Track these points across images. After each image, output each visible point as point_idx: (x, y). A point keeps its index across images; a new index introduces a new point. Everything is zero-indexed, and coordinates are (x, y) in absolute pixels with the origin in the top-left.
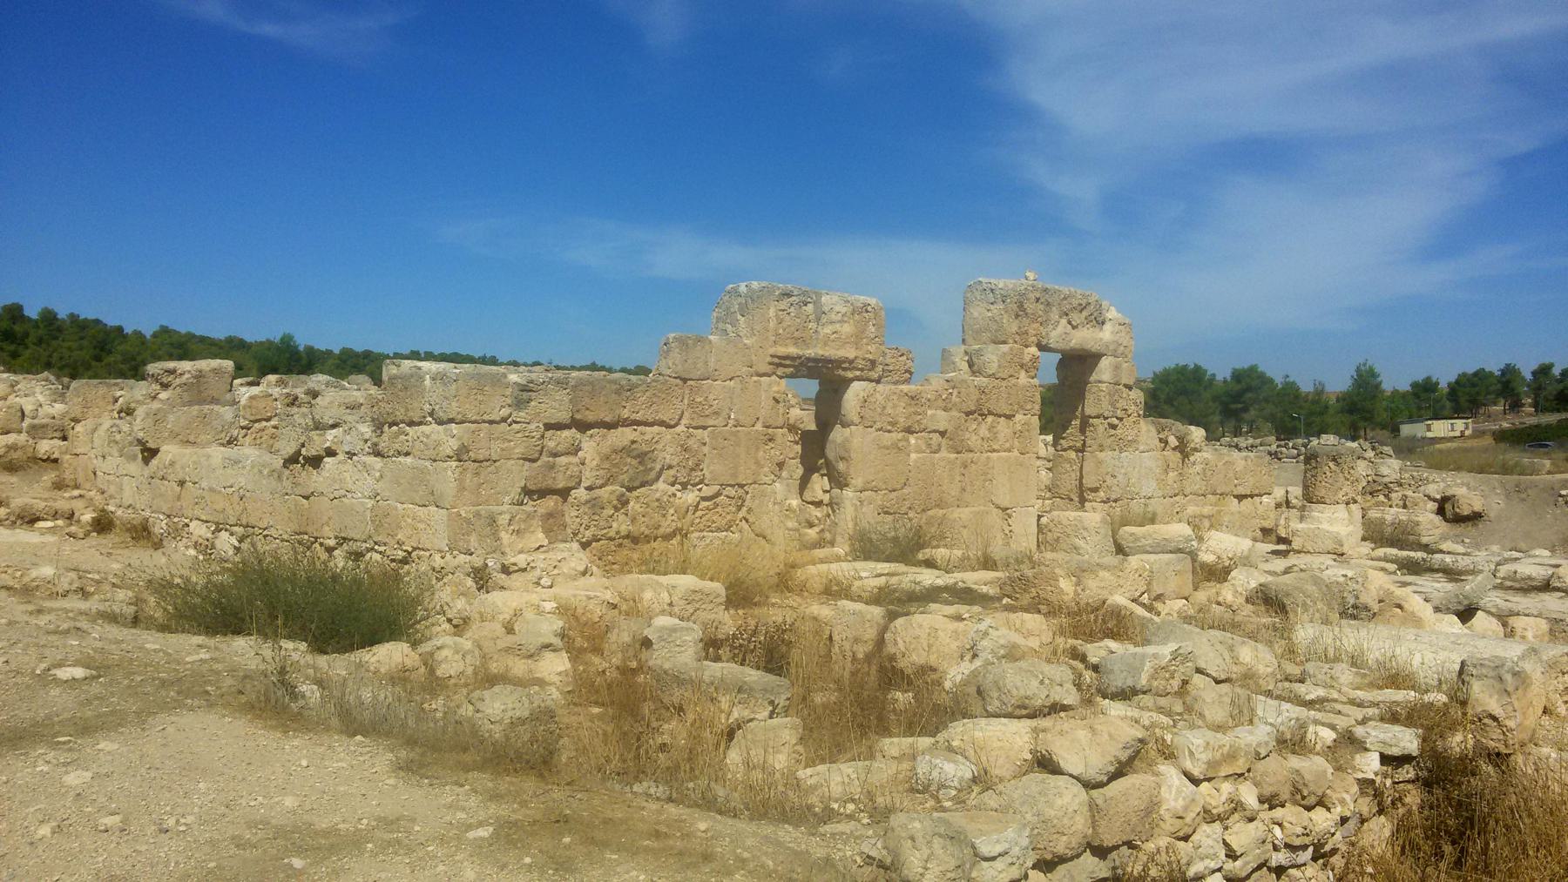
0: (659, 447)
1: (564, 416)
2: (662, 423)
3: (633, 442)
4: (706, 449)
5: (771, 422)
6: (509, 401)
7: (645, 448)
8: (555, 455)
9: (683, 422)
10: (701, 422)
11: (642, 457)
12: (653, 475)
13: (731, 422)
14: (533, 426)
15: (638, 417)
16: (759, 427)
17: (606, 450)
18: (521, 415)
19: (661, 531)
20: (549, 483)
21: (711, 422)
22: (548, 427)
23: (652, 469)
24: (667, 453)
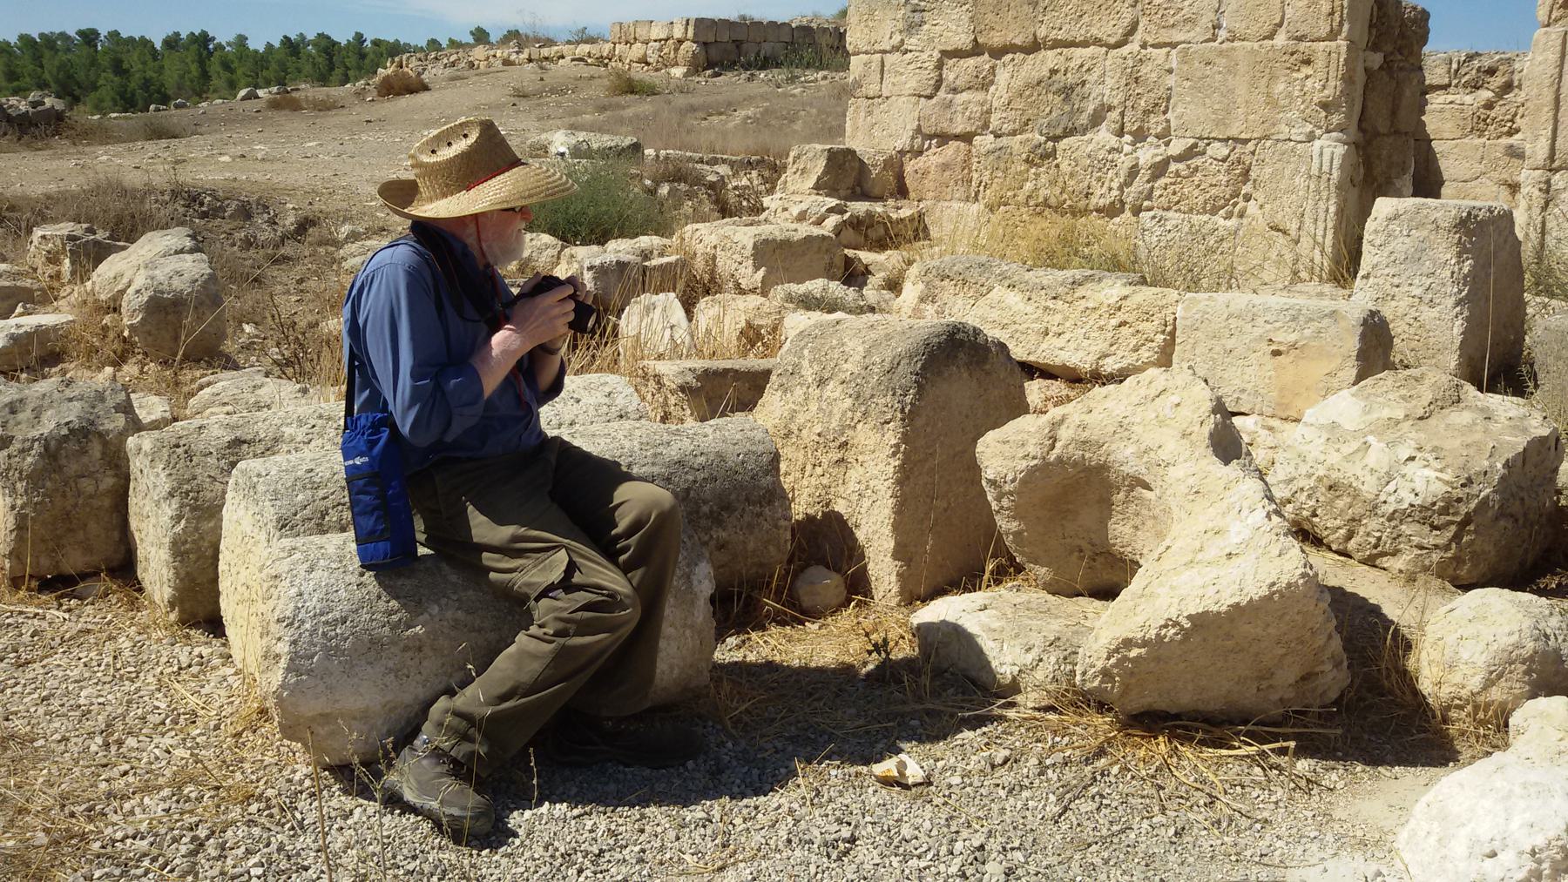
0: (1092, 77)
1: (963, 40)
2: (1097, 42)
3: (1054, 72)
4: (1171, 81)
5: (1304, 29)
6: (900, 25)
7: (1071, 79)
8: (955, 91)
9: (1138, 36)
10: (1164, 36)
11: (1067, 92)
12: (1083, 119)
13: (1223, 34)
14: (924, 56)
15: (1061, 35)
16: (1281, 40)
17: (1018, 83)
18: (911, 43)
19: (1094, 201)
20: (944, 126)
21: (1177, 36)
22: (944, 53)
23: (1080, 111)
24: (1105, 87)
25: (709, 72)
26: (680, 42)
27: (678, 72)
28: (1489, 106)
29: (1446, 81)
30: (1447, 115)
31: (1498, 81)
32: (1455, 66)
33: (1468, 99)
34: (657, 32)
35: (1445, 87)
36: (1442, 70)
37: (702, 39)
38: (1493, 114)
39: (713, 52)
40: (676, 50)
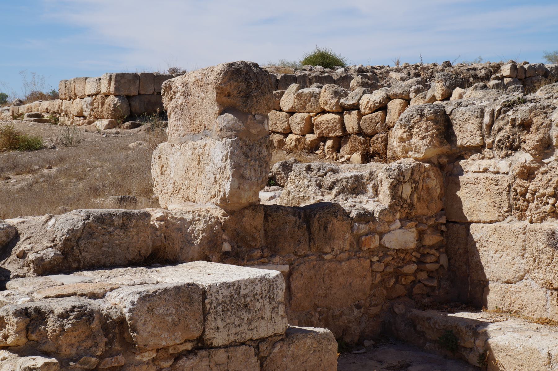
25: (128, 124)
26: (107, 96)
27: (101, 124)
28: (528, 174)
29: (477, 141)
30: (481, 188)
31: (532, 139)
32: (487, 119)
33: (503, 165)
34: (90, 89)
35: (479, 149)
36: (471, 126)
37: (126, 93)
38: (532, 187)
39: (137, 105)
40: (103, 104)
